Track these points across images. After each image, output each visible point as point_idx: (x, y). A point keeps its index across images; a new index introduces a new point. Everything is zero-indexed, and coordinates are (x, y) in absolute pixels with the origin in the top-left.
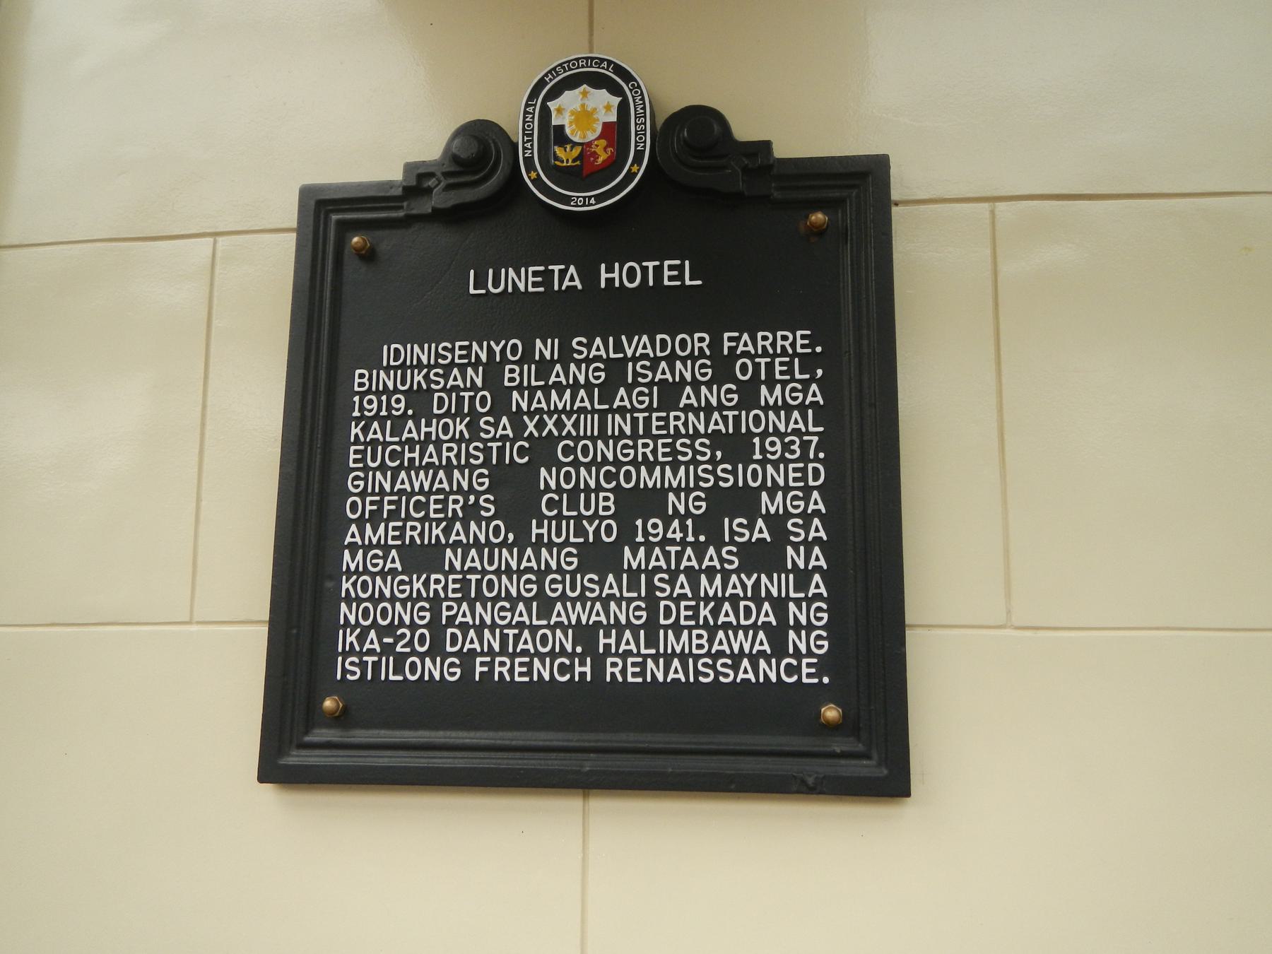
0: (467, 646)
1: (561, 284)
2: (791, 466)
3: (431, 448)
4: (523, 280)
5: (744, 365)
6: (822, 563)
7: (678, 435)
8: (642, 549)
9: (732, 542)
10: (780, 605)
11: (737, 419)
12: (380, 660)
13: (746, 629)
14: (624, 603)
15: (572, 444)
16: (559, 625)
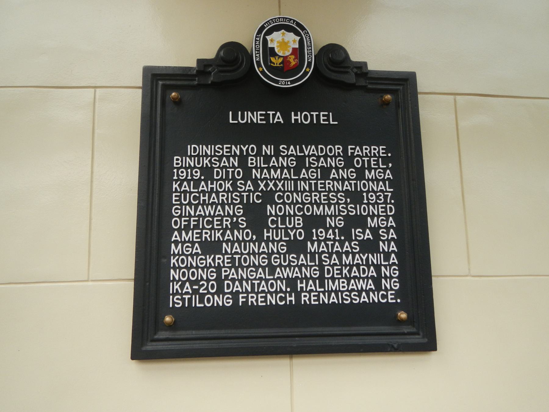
0: (235, 289)
1: (273, 120)
2: (380, 206)
3: (214, 195)
6: (395, 249)
8: (316, 243)
9: (356, 240)
10: (378, 268)
11: (356, 185)
12: (192, 297)
13: (363, 279)
14: (308, 268)
15: (282, 194)
16: (279, 278)
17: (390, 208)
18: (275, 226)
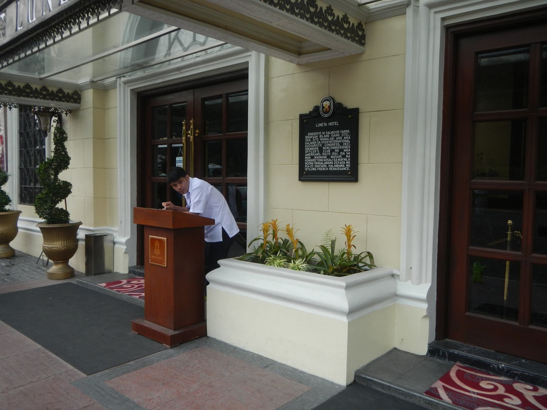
4: (321, 125)
10: (345, 162)
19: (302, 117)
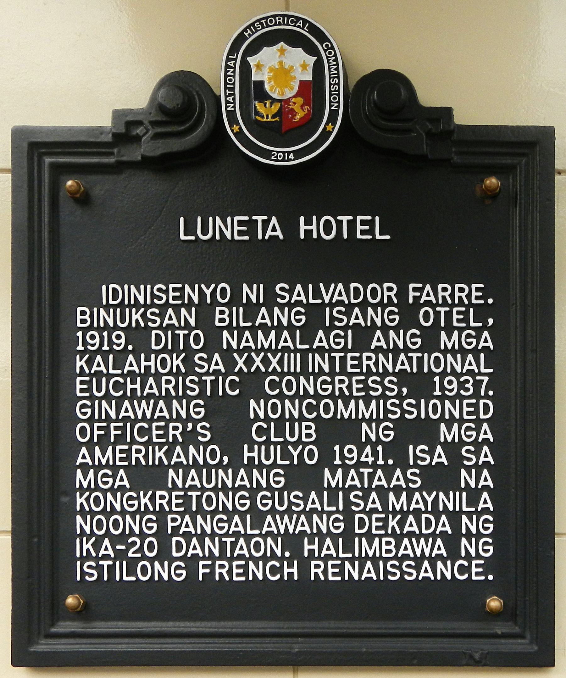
0: (191, 552)
1: (264, 234)
2: (465, 402)
3: (151, 380)
4: (230, 228)
5: (426, 313)
6: (490, 483)
7: (369, 373)
8: (340, 470)
9: (416, 465)
10: (454, 517)
11: (420, 360)
12: (114, 564)
13: (426, 537)
14: (325, 516)
15: (277, 379)
17: (485, 405)
18: (264, 438)
19: (44, 158)
